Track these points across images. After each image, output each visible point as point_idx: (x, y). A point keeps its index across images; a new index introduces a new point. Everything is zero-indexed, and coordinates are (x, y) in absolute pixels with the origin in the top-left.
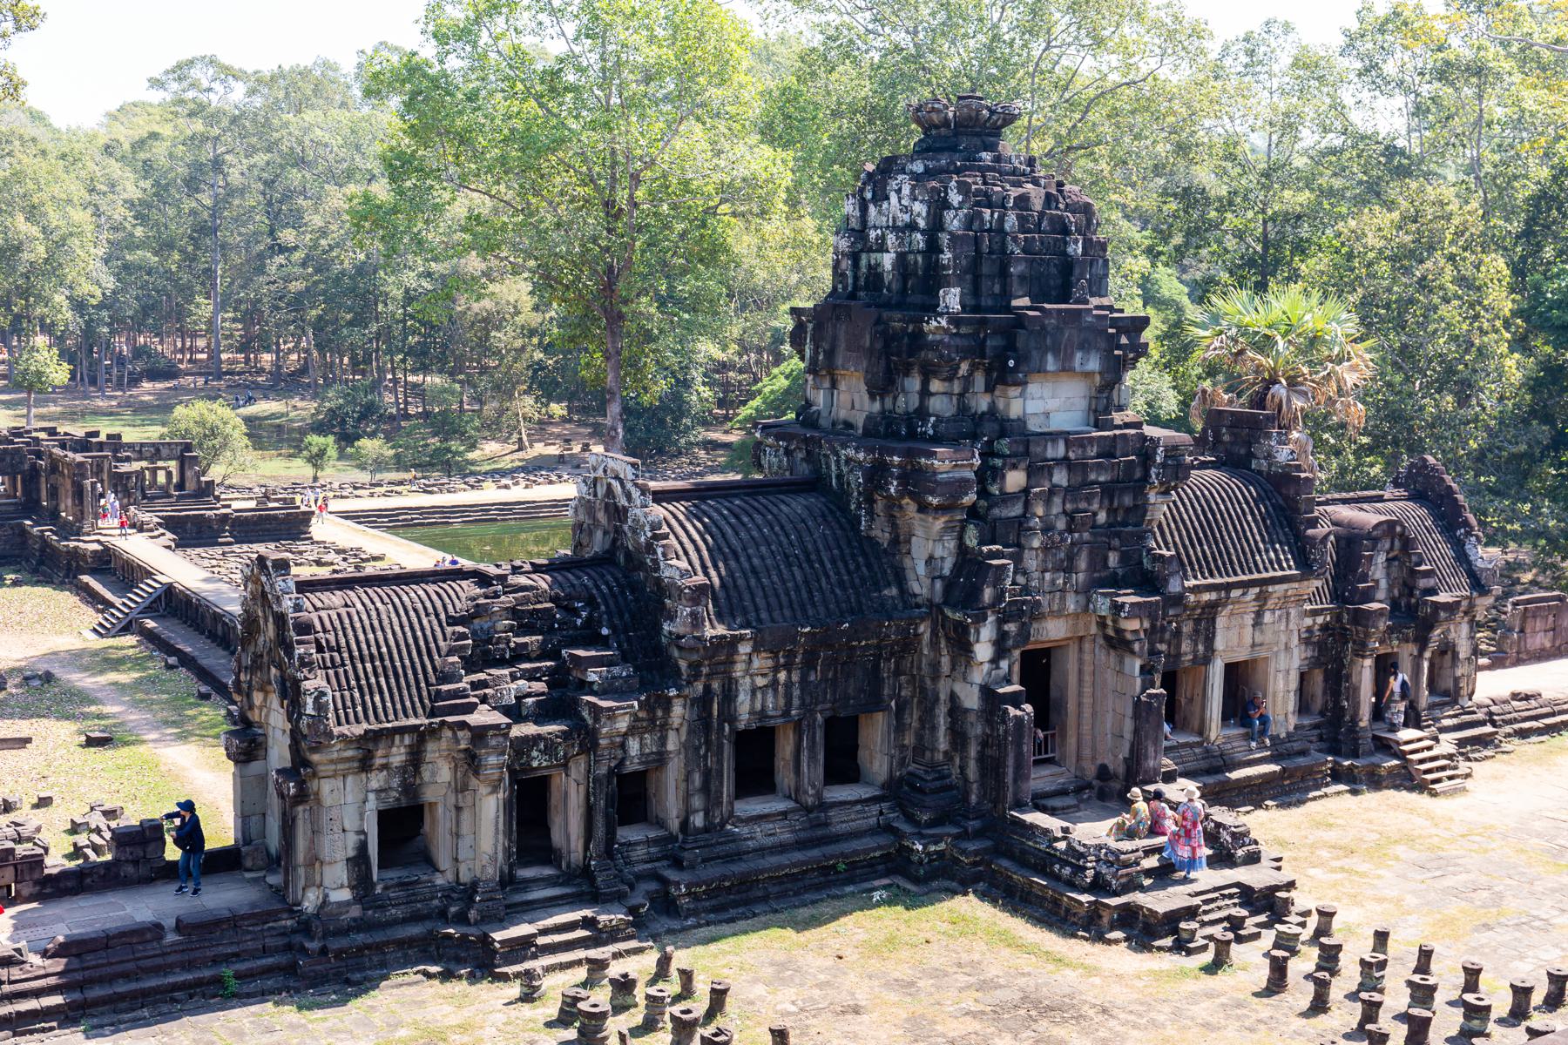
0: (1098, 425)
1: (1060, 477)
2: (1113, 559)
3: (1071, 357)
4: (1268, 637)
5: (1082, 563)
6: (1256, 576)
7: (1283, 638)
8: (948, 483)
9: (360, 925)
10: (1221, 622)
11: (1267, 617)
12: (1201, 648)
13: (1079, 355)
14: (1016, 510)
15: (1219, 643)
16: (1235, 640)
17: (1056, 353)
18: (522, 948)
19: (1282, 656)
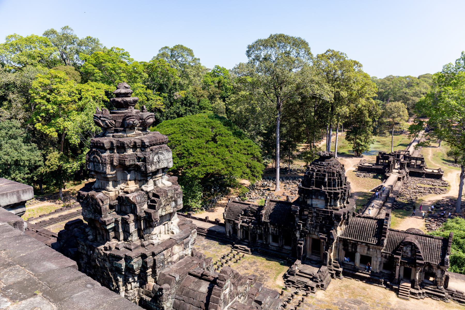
0: (326, 208)
1: (315, 214)
2: (324, 229)
3: (318, 197)
4: (371, 253)
5: (318, 228)
6: (366, 242)
7: (375, 255)
8: (294, 211)
9: (228, 238)
10: (359, 247)
11: (371, 250)
12: (353, 250)
13: (319, 197)
14: (306, 217)
15: (358, 250)
16: (362, 251)
17: (315, 196)
18: (237, 248)
19: (375, 258)
